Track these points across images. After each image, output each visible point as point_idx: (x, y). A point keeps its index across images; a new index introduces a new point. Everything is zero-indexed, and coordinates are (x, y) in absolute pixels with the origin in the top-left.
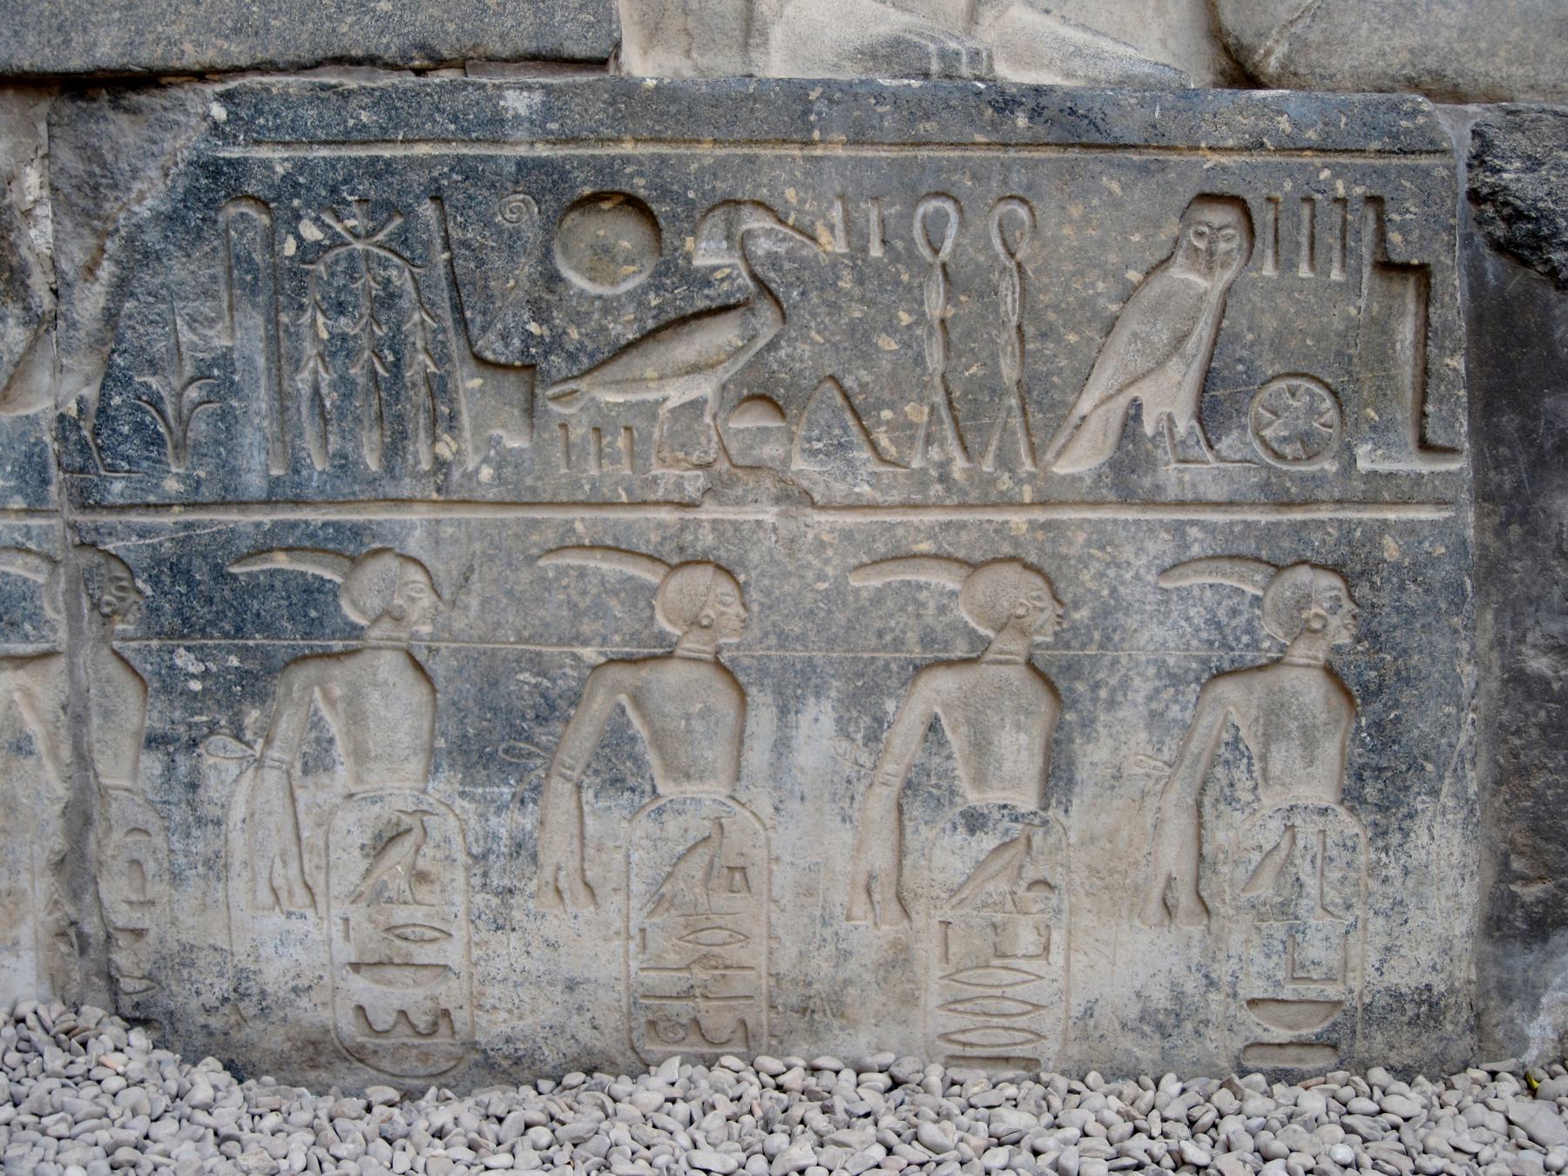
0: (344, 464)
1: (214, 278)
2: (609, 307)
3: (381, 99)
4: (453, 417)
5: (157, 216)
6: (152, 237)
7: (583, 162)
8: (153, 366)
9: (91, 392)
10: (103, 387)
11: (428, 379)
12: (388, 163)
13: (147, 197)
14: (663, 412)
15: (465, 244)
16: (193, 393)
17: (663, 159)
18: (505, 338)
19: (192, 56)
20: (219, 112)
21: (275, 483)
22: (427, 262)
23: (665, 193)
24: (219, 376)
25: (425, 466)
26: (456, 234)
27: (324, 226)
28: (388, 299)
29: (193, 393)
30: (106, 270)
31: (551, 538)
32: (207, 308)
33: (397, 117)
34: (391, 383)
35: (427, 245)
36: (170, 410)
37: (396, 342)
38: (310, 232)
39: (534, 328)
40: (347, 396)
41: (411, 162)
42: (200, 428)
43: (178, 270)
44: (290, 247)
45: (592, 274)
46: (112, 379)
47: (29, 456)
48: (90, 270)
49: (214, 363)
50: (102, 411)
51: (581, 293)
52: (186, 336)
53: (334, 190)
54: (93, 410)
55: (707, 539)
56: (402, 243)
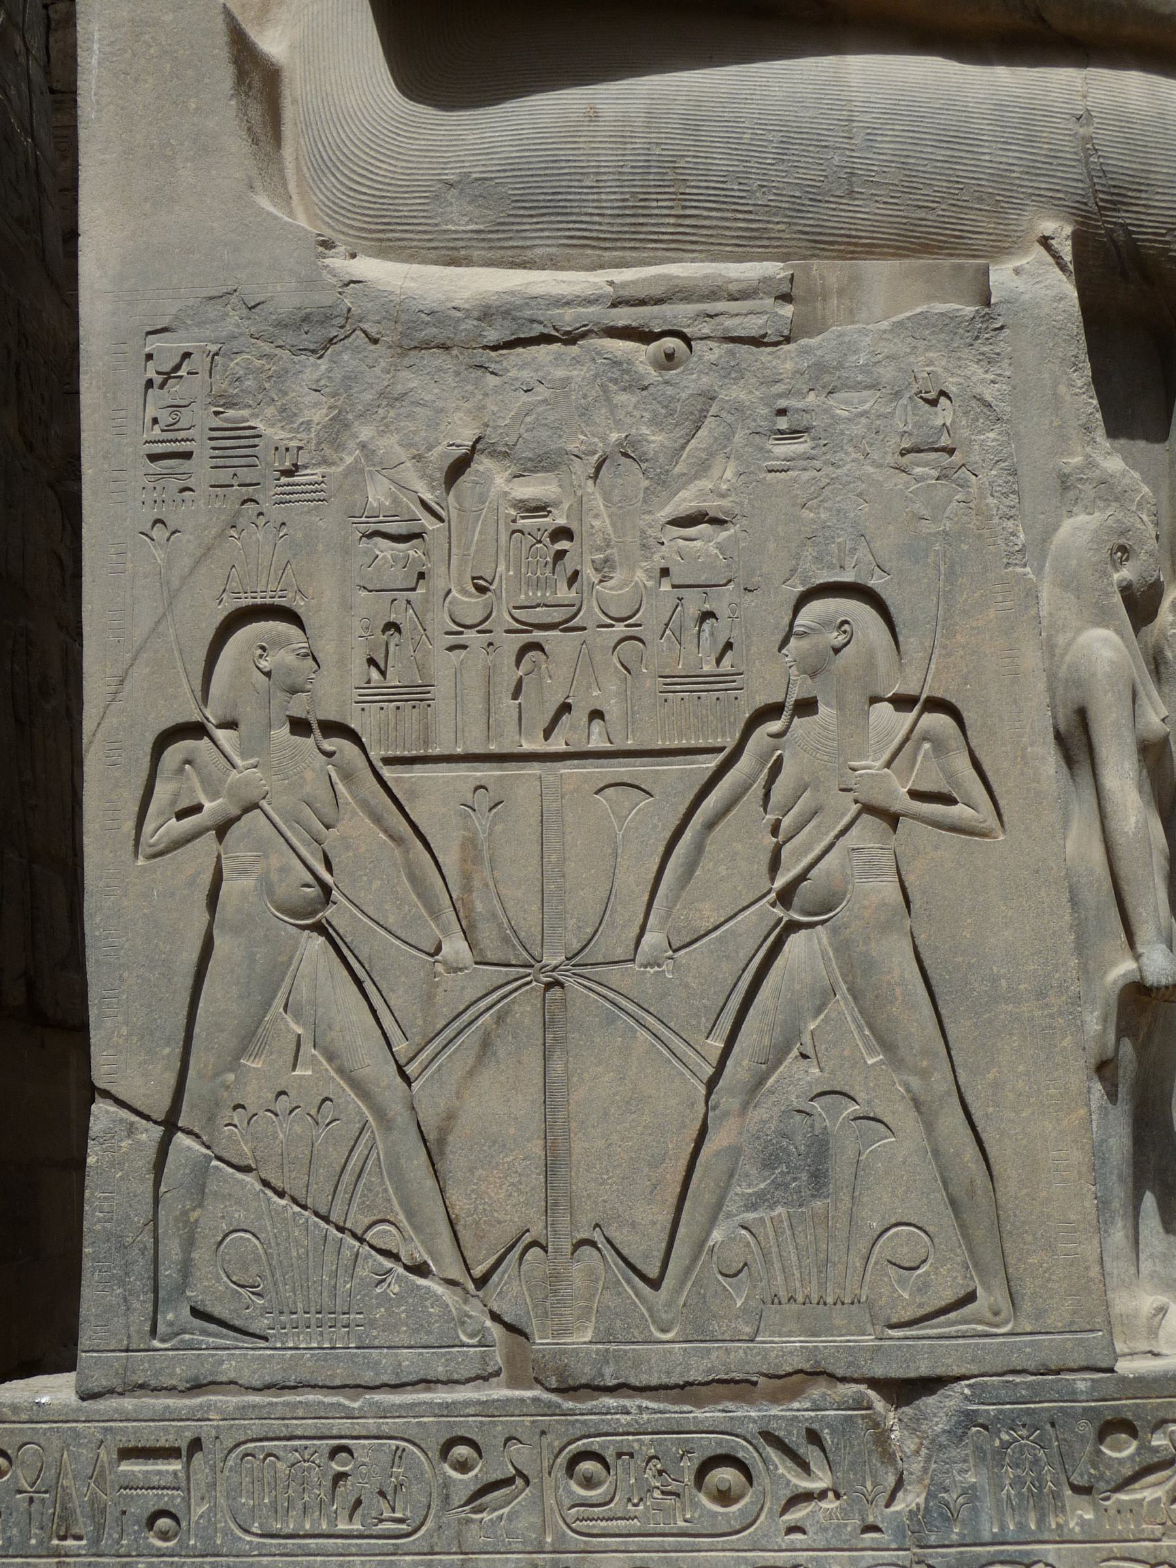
0: (1021, 1527)
1: (967, 1455)
2: (1121, 1461)
3: (1029, 1385)
4: (1063, 1506)
5: (944, 1431)
6: (943, 1439)
7: (1107, 1407)
8: (946, 1490)
9: (921, 1500)
10: (926, 1498)
11: (1052, 1492)
12: (1033, 1409)
13: (940, 1425)
14: (1145, 1504)
15: (1065, 1440)
16: (961, 1500)
17: (1138, 1405)
18: (1081, 1475)
19: (956, 1371)
20: (967, 1391)
21: (994, 1535)
22: (1050, 1447)
23: (1139, 1418)
24: (971, 1493)
25: (1054, 1526)
26: (1060, 1437)
27: (1010, 1435)
28: (1036, 1461)
29: (961, 1500)
30: (924, 1451)
31: (1105, 1555)
32: (965, 1466)
33: (1036, 1394)
34: (1039, 1496)
35: (1050, 1440)
36: (952, 1506)
37: (1040, 1478)
38: (1005, 1437)
39: (1092, 1471)
40: (1021, 1500)
41: (1042, 1409)
42: (964, 1514)
43: (954, 1453)
44: (997, 1443)
45: (1112, 1448)
46: (930, 1496)
47: (898, 1527)
48: (917, 1452)
49: (970, 1488)
50: (926, 1508)
51: (1110, 1457)
52: (958, 1478)
53: (1013, 1421)
54: (922, 1506)
55: (1166, 1553)
56: (1041, 1443)
